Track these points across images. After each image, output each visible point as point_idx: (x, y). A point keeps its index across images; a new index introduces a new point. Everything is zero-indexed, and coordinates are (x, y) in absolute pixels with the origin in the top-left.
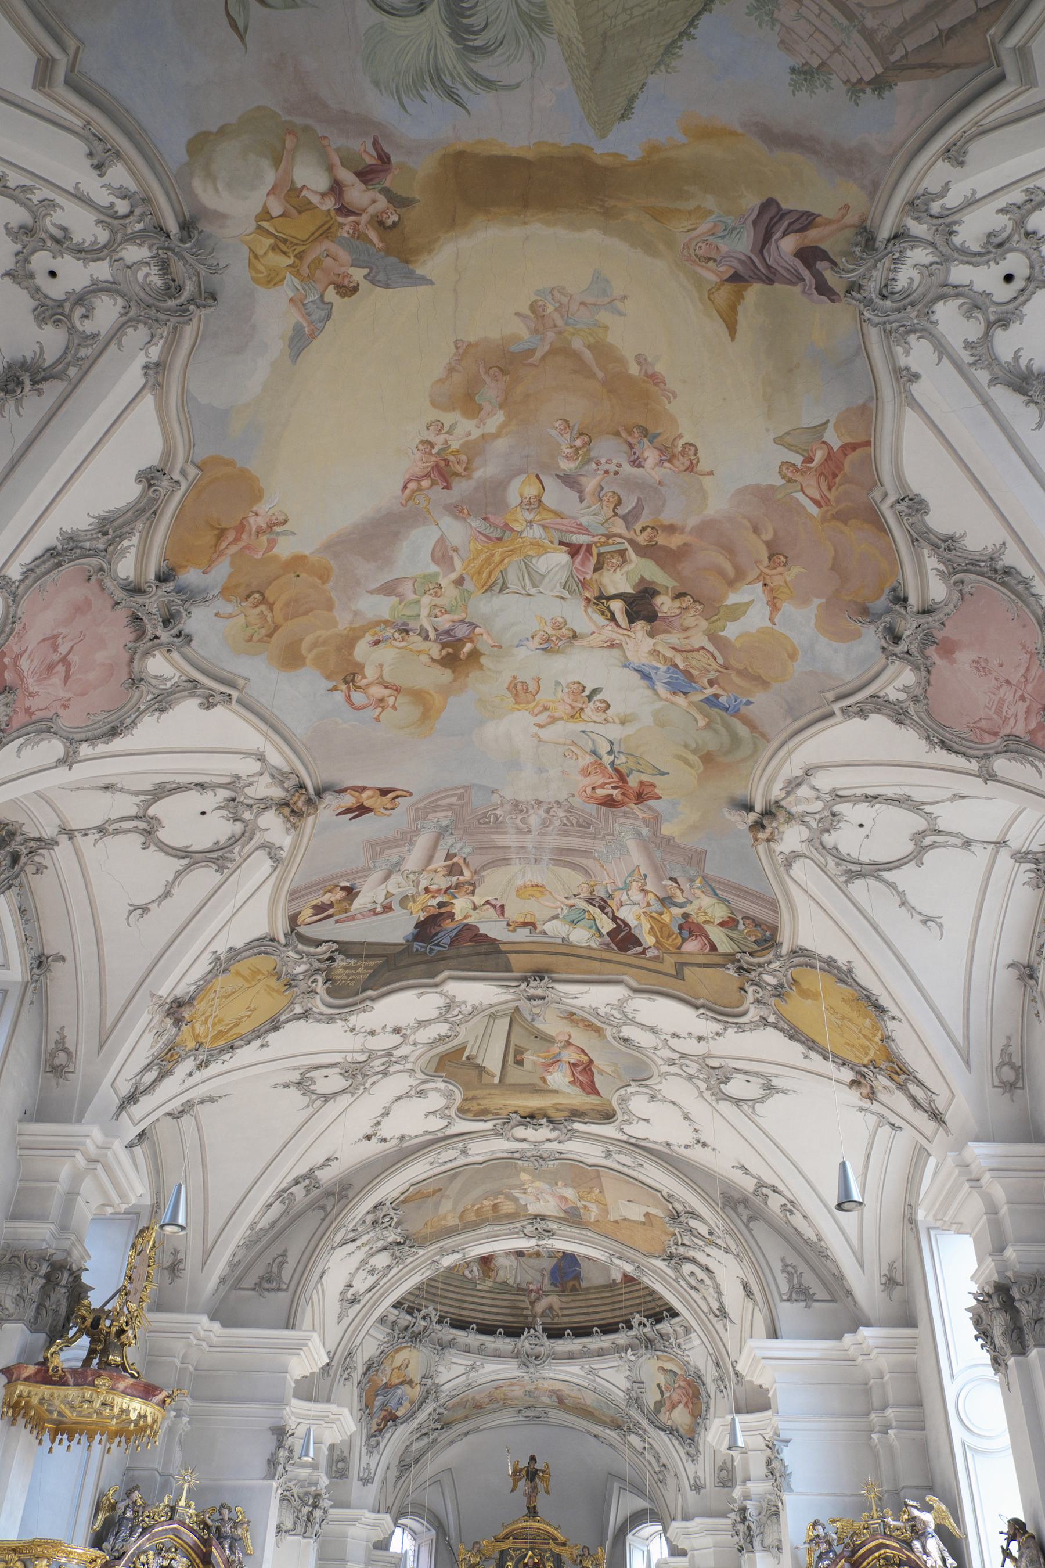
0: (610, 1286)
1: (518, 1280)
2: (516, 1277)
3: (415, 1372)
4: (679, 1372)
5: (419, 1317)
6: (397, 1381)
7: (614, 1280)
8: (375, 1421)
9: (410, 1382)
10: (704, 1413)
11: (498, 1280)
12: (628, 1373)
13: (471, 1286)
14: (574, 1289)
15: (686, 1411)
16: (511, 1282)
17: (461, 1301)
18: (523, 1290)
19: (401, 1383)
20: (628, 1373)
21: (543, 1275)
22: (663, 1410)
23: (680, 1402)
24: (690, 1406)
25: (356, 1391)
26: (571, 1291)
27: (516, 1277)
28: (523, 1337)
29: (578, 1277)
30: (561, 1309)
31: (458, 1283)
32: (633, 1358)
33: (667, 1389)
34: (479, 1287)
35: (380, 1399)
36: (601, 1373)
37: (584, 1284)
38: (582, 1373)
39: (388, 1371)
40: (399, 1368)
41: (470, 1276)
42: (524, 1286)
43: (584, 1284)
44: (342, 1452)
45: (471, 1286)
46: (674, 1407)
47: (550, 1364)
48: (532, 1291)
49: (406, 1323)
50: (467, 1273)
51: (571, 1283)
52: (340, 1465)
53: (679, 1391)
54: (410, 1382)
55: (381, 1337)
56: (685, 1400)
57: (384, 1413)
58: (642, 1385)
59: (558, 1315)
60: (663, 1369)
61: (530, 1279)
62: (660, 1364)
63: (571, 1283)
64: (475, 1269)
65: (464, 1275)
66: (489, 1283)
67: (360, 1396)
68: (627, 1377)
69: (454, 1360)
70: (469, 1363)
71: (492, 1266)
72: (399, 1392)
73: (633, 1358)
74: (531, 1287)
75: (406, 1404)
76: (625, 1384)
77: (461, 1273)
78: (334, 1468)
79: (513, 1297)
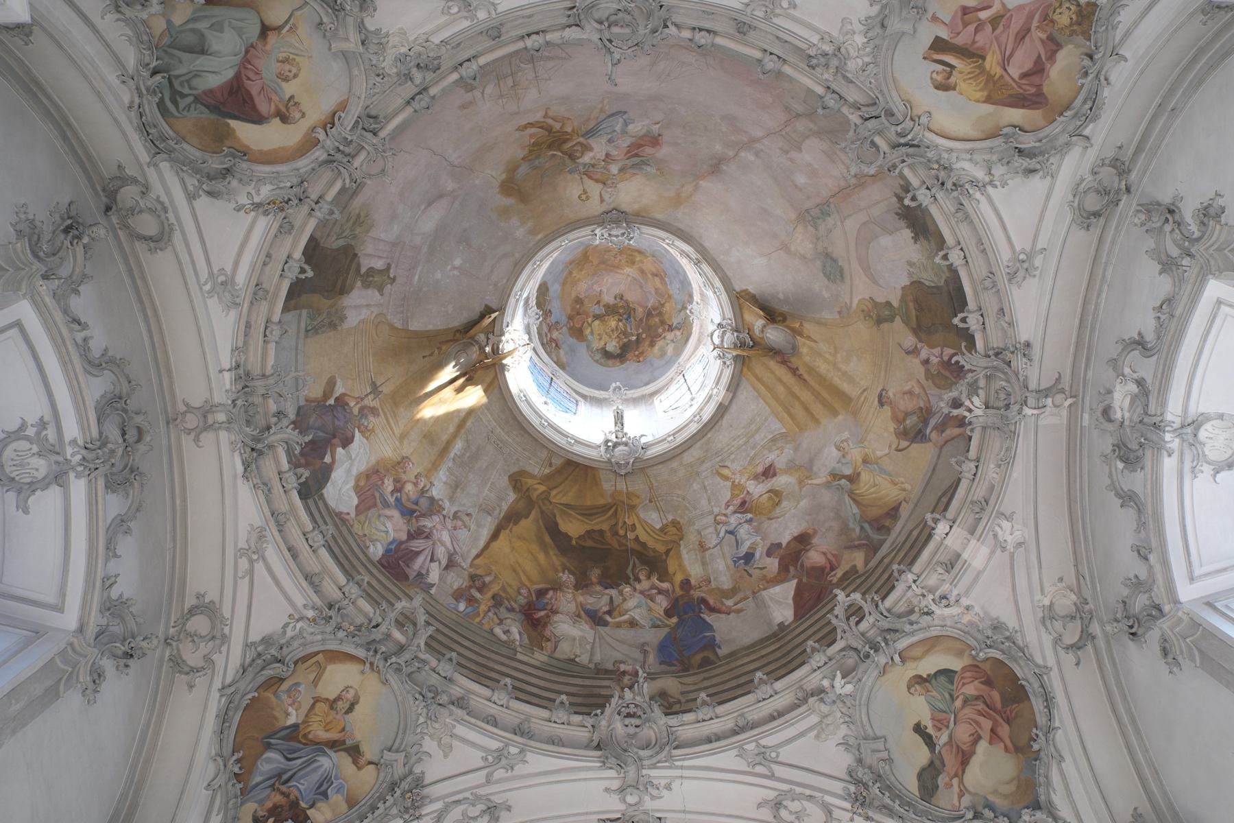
0: (775, 635)
1: (597, 658)
2: (592, 653)
4: (956, 664)
5: (392, 615)
6: (323, 735)
7: (781, 625)
9: (354, 752)
10: (1041, 720)
11: (557, 655)
12: (843, 730)
13: (504, 651)
14: (706, 662)
15: (998, 750)
16: (584, 659)
18: (607, 672)
19: (334, 745)
20: (843, 730)
21: (645, 652)
22: (941, 780)
23: (977, 739)
24: (1004, 730)
26: (700, 666)
27: (592, 653)
28: (608, 710)
29: (711, 645)
30: (682, 693)
31: (481, 641)
32: (849, 688)
33: (940, 724)
34: (519, 656)
35: (271, 761)
36: (785, 754)
37: (722, 652)
38: (743, 767)
40: (332, 704)
41: (504, 637)
42: (610, 666)
43: (722, 652)
45: (504, 651)
46: (965, 758)
47: (670, 758)
48: (624, 673)
49: (360, 620)
50: (498, 631)
51: (701, 656)
53: (968, 712)
55: (299, 601)
56: (987, 724)
57: (277, 798)
58: (880, 745)
59: (679, 702)
60: (919, 680)
61: (619, 657)
62: (912, 669)
63: (701, 656)
64: (515, 630)
65: (491, 632)
66: (540, 657)
67: (223, 719)
68: (845, 744)
69: (460, 730)
70: (495, 745)
71: (547, 633)
72: (325, 763)
73: (849, 688)
74: (623, 667)
75: (337, 799)
76: (840, 761)
77: (486, 627)
79: (587, 682)
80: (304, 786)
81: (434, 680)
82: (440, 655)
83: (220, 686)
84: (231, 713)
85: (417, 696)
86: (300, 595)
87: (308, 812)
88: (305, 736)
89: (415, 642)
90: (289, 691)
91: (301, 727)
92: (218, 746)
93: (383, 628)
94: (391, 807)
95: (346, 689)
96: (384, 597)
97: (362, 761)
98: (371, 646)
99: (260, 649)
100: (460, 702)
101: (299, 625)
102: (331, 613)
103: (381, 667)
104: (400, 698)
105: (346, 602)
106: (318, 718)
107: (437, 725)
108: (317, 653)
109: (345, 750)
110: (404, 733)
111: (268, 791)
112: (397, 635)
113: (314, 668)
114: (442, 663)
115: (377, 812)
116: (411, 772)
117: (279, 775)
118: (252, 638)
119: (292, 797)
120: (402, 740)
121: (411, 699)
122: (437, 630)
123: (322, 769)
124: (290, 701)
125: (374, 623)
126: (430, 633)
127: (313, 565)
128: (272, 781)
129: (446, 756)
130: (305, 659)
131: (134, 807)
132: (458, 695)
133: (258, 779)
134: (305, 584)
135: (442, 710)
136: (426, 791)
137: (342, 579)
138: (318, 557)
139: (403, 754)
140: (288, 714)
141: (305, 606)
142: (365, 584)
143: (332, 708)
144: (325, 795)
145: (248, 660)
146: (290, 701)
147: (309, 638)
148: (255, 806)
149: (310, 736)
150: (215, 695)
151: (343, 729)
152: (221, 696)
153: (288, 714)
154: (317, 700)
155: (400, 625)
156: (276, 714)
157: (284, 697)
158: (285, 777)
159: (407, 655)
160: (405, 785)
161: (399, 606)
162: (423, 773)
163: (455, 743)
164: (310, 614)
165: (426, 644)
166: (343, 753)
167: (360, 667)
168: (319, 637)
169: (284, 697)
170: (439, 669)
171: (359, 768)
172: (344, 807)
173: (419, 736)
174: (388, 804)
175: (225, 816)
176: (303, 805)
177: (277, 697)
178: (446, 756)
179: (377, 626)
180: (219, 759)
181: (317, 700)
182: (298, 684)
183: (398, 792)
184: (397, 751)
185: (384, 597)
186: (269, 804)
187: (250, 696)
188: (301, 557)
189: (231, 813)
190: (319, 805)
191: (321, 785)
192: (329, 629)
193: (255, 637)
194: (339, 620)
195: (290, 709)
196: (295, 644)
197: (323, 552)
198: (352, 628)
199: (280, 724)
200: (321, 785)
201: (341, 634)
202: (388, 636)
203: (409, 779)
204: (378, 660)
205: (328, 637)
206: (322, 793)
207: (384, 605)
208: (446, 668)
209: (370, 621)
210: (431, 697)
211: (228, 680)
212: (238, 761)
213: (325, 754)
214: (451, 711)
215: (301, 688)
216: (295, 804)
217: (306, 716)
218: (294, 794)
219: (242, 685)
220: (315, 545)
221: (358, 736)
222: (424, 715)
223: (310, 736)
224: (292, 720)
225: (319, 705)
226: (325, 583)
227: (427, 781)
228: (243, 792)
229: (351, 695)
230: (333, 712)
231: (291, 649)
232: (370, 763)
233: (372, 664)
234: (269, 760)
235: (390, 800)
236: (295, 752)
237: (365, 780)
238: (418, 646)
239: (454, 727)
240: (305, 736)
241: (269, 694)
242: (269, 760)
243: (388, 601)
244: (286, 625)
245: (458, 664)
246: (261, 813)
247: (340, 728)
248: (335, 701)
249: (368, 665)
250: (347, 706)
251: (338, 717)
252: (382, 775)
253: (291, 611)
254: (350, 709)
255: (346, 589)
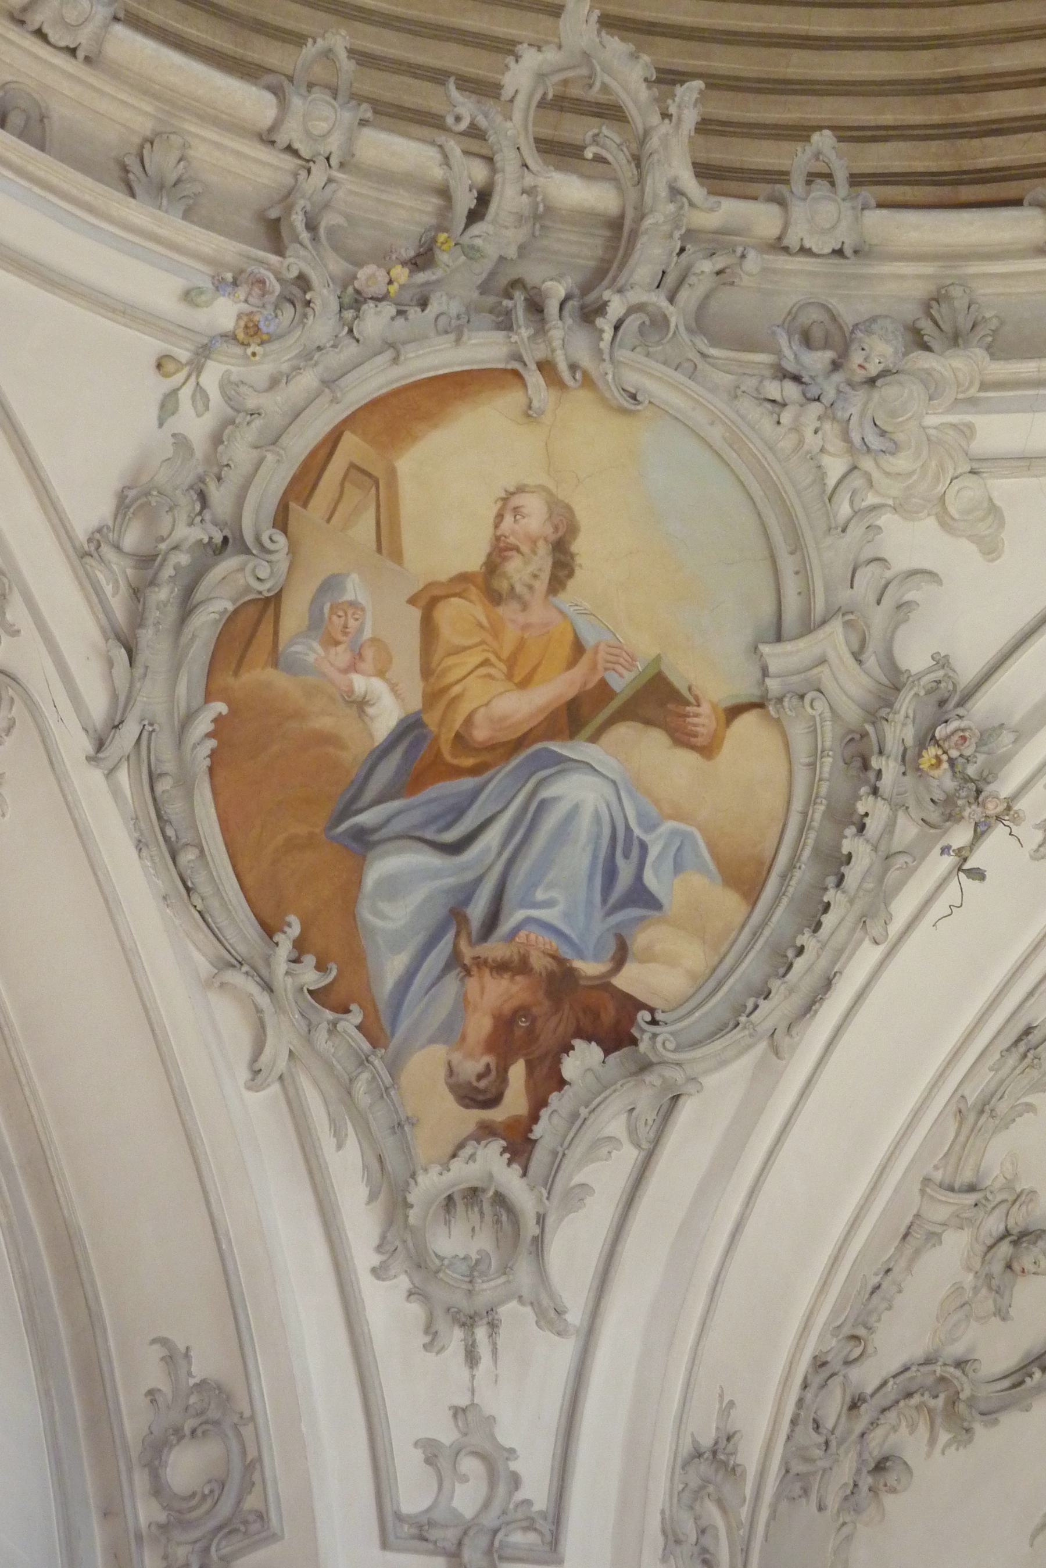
3: (658, 586)
5: (513, 130)
6: (521, 706)
8: (427, 1067)
9: (658, 702)
17: (959, 85)
19: (574, 717)
25: (107, 806)
35: (401, 888)
39: (384, 614)
40: (489, 582)
44: (174, 1358)
49: (408, 216)
52: (186, 1467)
54: (658, 702)
57: (497, 992)
67: (166, 841)
69: (998, 431)
75: (689, 889)
78: (145, 1512)
80: (556, 908)
81: (798, 283)
82: (769, 183)
83: (85, 745)
84: (174, 809)
85: (773, 389)
86: (150, 269)
87: (620, 982)
88: (461, 741)
89: (656, 184)
90: (316, 623)
91: (432, 720)
92: (203, 936)
93: (508, 200)
94: (890, 827)
95: (508, 504)
96: (438, 77)
97: (704, 719)
98: (511, 299)
99: (132, 538)
100: (936, 325)
101: (211, 377)
102: (295, 262)
103: (586, 361)
104: (716, 434)
105: (319, 174)
106: (474, 658)
107: (902, 462)
108: (333, 440)
109: (625, 714)
110: (797, 547)
111: (451, 984)
112: (572, 191)
113: (353, 495)
114: (798, 210)
115: (853, 874)
116: (894, 682)
117: (457, 916)
118: (81, 531)
119: (539, 963)
120: (803, 572)
121: (760, 417)
122: (715, 83)
123: (585, 822)
124: (341, 656)
125: (465, 201)
126: (690, 117)
127: (106, 111)
128: (444, 947)
129: (991, 550)
130: (304, 483)
131: (66, 1245)
132: (921, 290)
133: (392, 967)
134: (137, 213)
135: (888, 391)
136: (982, 706)
137: (254, 103)
138: (116, 73)
139: (836, 627)
140: (361, 705)
141: (189, 296)
142: (347, 65)
143: (495, 598)
144: (641, 897)
145: (118, 604)
146: (341, 656)
147: (275, 404)
148: (439, 1052)
149: (481, 734)
150: (89, 782)
151: (578, 648)
152: (110, 774)
153: (361, 705)
154: (429, 602)
155: (559, 152)
156: (324, 723)
157: (311, 652)
158: (477, 911)
159: (650, 255)
160: (899, 731)
161: (520, 77)
162: (942, 662)
163: (1003, 487)
164: (224, 313)
165: (704, 171)
166: (624, 731)
167: (511, 399)
168: (308, 380)
169: (311, 652)
170: (798, 234)
171: (708, 750)
172: (731, 902)
173: (856, 531)
174: (873, 826)
175: (366, 1132)
176: (590, 968)
177: (294, 668)
178: (991, 550)
179: (484, 198)
180: (236, 977)
181: (429, 602)
182: (331, 585)
183: (890, 769)
184: (808, 626)
185: (438, 77)
186: (480, 1026)
187: (203, 725)
188: (60, 111)
189: (379, 1120)
190: (640, 940)
191: (611, 874)
192: (322, 325)
193: (89, 509)
194: (336, 265)
195: (360, 683)
196: (240, 452)
197: (130, 46)
198: (401, 273)
199: (355, 752)
200: (611, 874)
201: (375, 321)
202: (542, 216)
203: (905, 704)
204: (567, 341)
205: (333, 360)
206: (626, 893)
207: (466, 108)
208: (822, 218)
209: (444, 193)
210: (821, 355)
211: (98, 705)
212: (300, 946)
213: (562, 764)
214: (926, 378)
215: (354, 589)
216: (561, 981)
217: (426, 672)
218: (539, 946)
219: (152, 697)
220: (83, 38)
221: (644, 647)
222: (836, 444)
223: (481, 734)
224: (386, 716)
225: (448, 613)
226: (200, 152)
227: (967, 671)
228: (373, 1032)
229: (535, 518)
230: (508, 611)
231: (234, 478)
232: (734, 712)
233: (546, 367)
234: (392, 888)
235: (876, 812)
236: (458, 812)
237: (752, 776)
238: (675, 192)
239: (967, 431)
240: (461, 741)
241: (258, 675)
242: (392, 888)
243: (469, 85)
244: (168, 405)
245: (857, 180)
246: (471, 1067)
247: (565, 651)
248: (493, 566)
249: (535, 379)
250: (543, 561)
251: (538, 613)
252: (798, 733)
253: (155, 346)
254: (562, 566)
255: (291, 132)
